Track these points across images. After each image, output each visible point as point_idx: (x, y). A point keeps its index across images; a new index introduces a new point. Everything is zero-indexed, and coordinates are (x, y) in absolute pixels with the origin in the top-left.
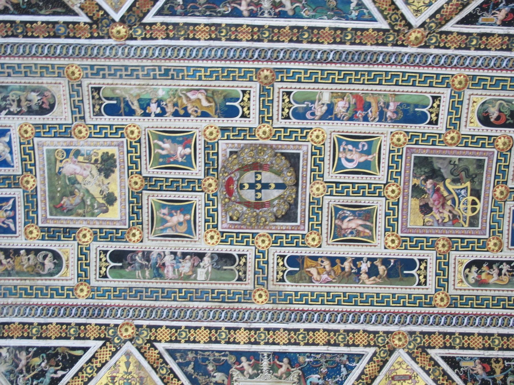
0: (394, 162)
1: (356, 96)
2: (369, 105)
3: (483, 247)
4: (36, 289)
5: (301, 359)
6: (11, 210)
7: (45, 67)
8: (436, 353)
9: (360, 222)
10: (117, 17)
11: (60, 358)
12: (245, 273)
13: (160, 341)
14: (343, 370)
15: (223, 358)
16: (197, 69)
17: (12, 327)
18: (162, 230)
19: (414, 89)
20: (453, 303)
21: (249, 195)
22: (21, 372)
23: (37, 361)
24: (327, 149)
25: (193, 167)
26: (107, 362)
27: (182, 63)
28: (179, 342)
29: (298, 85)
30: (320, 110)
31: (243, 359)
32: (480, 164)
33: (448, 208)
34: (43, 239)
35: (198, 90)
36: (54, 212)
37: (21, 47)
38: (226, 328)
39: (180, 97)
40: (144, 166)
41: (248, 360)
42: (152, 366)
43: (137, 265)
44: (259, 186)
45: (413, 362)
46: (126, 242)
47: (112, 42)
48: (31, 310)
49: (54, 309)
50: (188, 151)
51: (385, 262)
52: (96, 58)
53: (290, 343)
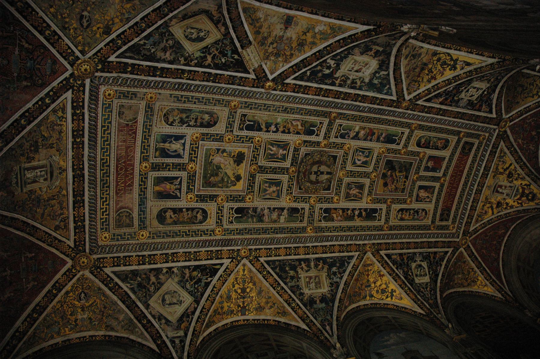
0: (377, 161)
1: (370, 129)
2: (374, 134)
3: (405, 202)
6: (178, 185)
8: (382, 253)
9: (358, 191)
10: (271, 77)
11: (208, 270)
12: (303, 218)
13: (261, 257)
16: (302, 109)
17: (179, 255)
18: (264, 195)
19: (395, 128)
20: (391, 228)
22: (187, 281)
23: (195, 273)
24: (350, 154)
25: (285, 161)
26: (234, 270)
28: (271, 256)
29: (346, 122)
30: (352, 134)
31: (302, 263)
32: (411, 164)
33: (395, 184)
34: (197, 202)
35: (298, 120)
36: (205, 186)
37: (208, 88)
38: (294, 247)
39: (288, 123)
40: (260, 160)
41: (305, 263)
42: (258, 270)
44: (319, 173)
45: (373, 258)
46: (245, 202)
47: (263, 90)
48: (189, 244)
49: (203, 243)
50: (285, 152)
51: (366, 210)
52: (250, 98)
53: (323, 253)
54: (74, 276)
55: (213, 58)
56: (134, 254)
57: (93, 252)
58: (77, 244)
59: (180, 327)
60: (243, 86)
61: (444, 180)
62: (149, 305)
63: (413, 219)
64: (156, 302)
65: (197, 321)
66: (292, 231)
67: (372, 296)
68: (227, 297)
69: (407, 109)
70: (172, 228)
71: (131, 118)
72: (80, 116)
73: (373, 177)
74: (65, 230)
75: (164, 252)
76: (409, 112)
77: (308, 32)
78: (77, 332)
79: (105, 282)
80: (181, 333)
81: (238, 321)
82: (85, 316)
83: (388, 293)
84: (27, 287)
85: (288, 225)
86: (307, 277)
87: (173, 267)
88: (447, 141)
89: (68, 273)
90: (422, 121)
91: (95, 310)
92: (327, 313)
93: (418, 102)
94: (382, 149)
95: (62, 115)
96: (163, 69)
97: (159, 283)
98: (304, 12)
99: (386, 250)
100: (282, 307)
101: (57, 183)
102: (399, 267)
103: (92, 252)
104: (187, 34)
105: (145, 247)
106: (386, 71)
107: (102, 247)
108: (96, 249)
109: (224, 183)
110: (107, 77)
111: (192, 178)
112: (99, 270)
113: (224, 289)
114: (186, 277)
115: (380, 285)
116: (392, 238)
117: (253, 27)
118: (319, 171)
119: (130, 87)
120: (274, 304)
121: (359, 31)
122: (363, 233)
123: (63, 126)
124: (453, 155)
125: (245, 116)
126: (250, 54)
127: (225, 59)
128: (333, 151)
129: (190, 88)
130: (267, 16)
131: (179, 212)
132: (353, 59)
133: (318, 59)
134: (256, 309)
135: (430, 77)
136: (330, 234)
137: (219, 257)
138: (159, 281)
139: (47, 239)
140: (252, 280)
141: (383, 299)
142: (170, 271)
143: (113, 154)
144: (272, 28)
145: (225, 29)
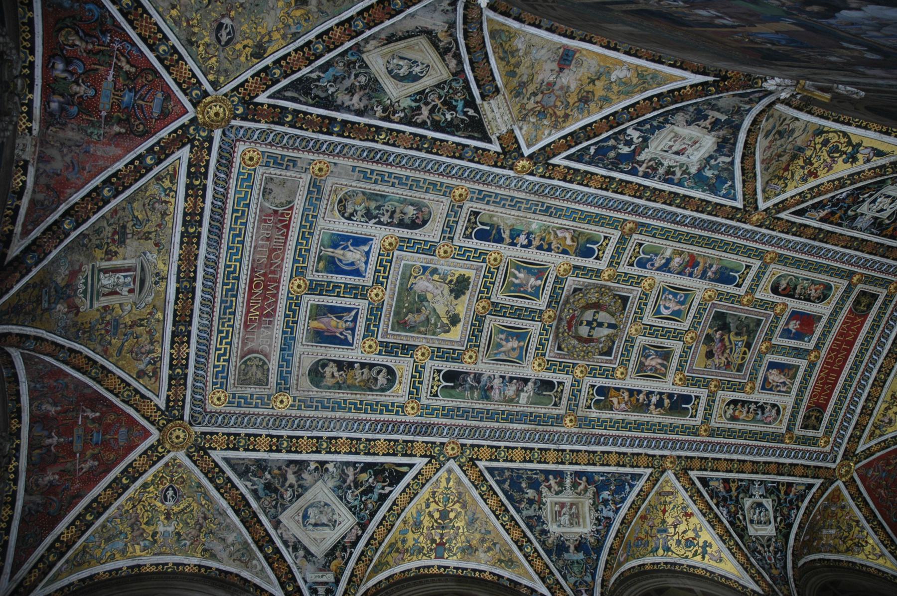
0: (699, 313)
1: (692, 256)
2: (698, 264)
3: (742, 389)
4: (366, 404)
5: (596, 478)
6: (351, 321)
7: (434, 184)
8: (693, 474)
9: (660, 361)
10: (527, 152)
11: (387, 474)
12: (560, 399)
13: (481, 460)
14: (627, 487)
15: (534, 476)
16: (575, 211)
17: (340, 441)
18: (496, 354)
19: (735, 257)
20: (712, 433)
21: (584, 331)
22: (349, 488)
23: (364, 477)
24: (653, 296)
26: (431, 478)
27: (566, 204)
29: (651, 239)
30: (659, 262)
31: (551, 477)
33: (726, 355)
34: (380, 354)
35: (567, 229)
36: (396, 328)
37: (419, 161)
38: (539, 449)
39: (550, 233)
40: (495, 292)
41: (555, 478)
42: (473, 483)
43: (467, 386)
44: (595, 324)
45: (676, 482)
46: (462, 362)
47: (511, 173)
48: (359, 425)
49: (382, 426)
50: (539, 282)
51: (670, 396)
53: (589, 464)
54: (160, 458)
55: (432, 111)
56: (264, 432)
57: (195, 421)
58: (171, 404)
59: (329, 567)
60: (479, 162)
61: (816, 357)
62: (279, 522)
63: (754, 420)
64: (292, 518)
65: (359, 559)
66: (537, 420)
67: (667, 549)
68: (415, 523)
69: (760, 226)
70: (332, 394)
71: (283, 201)
72: (199, 189)
73: (689, 339)
74: (153, 380)
75: (315, 433)
76: (763, 230)
77: (598, 79)
78: (155, 555)
79: (210, 475)
80: (329, 577)
81: (428, 567)
82: (171, 529)
83: (696, 548)
84: (82, 469)
85: (532, 410)
86: (556, 504)
87: (327, 462)
88: (828, 287)
89: (150, 453)
90: (785, 247)
91: (189, 521)
92: (586, 571)
93: (779, 215)
94: (709, 293)
95: (170, 185)
96: (344, 123)
97: (300, 486)
98: (595, 44)
99: (701, 470)
100: (508, 551)
101: (150, 299)
102: (722, 504)
103: (193, 421)
104: (391, 67)
105: (284, 422)
106: (729, 156)
107: (212, 414)
108: (201, 417)
109: (429, 326)
110: (250, 128)
111: (375, 312)
112: (202, 453)
113: (411, 510)
114: (348, 481)
115: (684, 532)
116: (713, 451)
117: (504, 63)
118: (596, 320)
119: (288, 149)
120: (494, 544)
121: (688, 84)
122: (662, 436)
123: (169, 205)
124: (835, 312)
125: (476, 214)
126: (496, 110)
127: (452, 114)
128: (623, 289)
129: (387, 159)
130: (530, 46)
131: (348, 368)
132: (672, 131)
133: (612, 128)
134: (463, 550)
135: (806, 172)
136: (605, 432)
137: (409, 452)
138: (300, 482)
139: (122, 390)
140: (459, 498)
141: (687, 557)
142: (322, 467)
143: (247, 258)
144: (537, 67)
145: (457, 65)
